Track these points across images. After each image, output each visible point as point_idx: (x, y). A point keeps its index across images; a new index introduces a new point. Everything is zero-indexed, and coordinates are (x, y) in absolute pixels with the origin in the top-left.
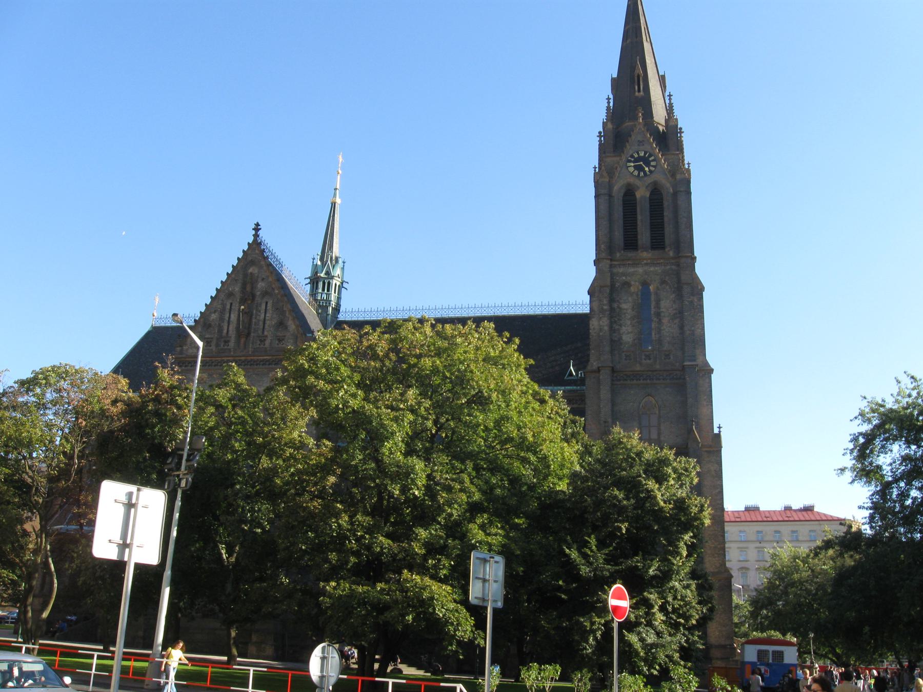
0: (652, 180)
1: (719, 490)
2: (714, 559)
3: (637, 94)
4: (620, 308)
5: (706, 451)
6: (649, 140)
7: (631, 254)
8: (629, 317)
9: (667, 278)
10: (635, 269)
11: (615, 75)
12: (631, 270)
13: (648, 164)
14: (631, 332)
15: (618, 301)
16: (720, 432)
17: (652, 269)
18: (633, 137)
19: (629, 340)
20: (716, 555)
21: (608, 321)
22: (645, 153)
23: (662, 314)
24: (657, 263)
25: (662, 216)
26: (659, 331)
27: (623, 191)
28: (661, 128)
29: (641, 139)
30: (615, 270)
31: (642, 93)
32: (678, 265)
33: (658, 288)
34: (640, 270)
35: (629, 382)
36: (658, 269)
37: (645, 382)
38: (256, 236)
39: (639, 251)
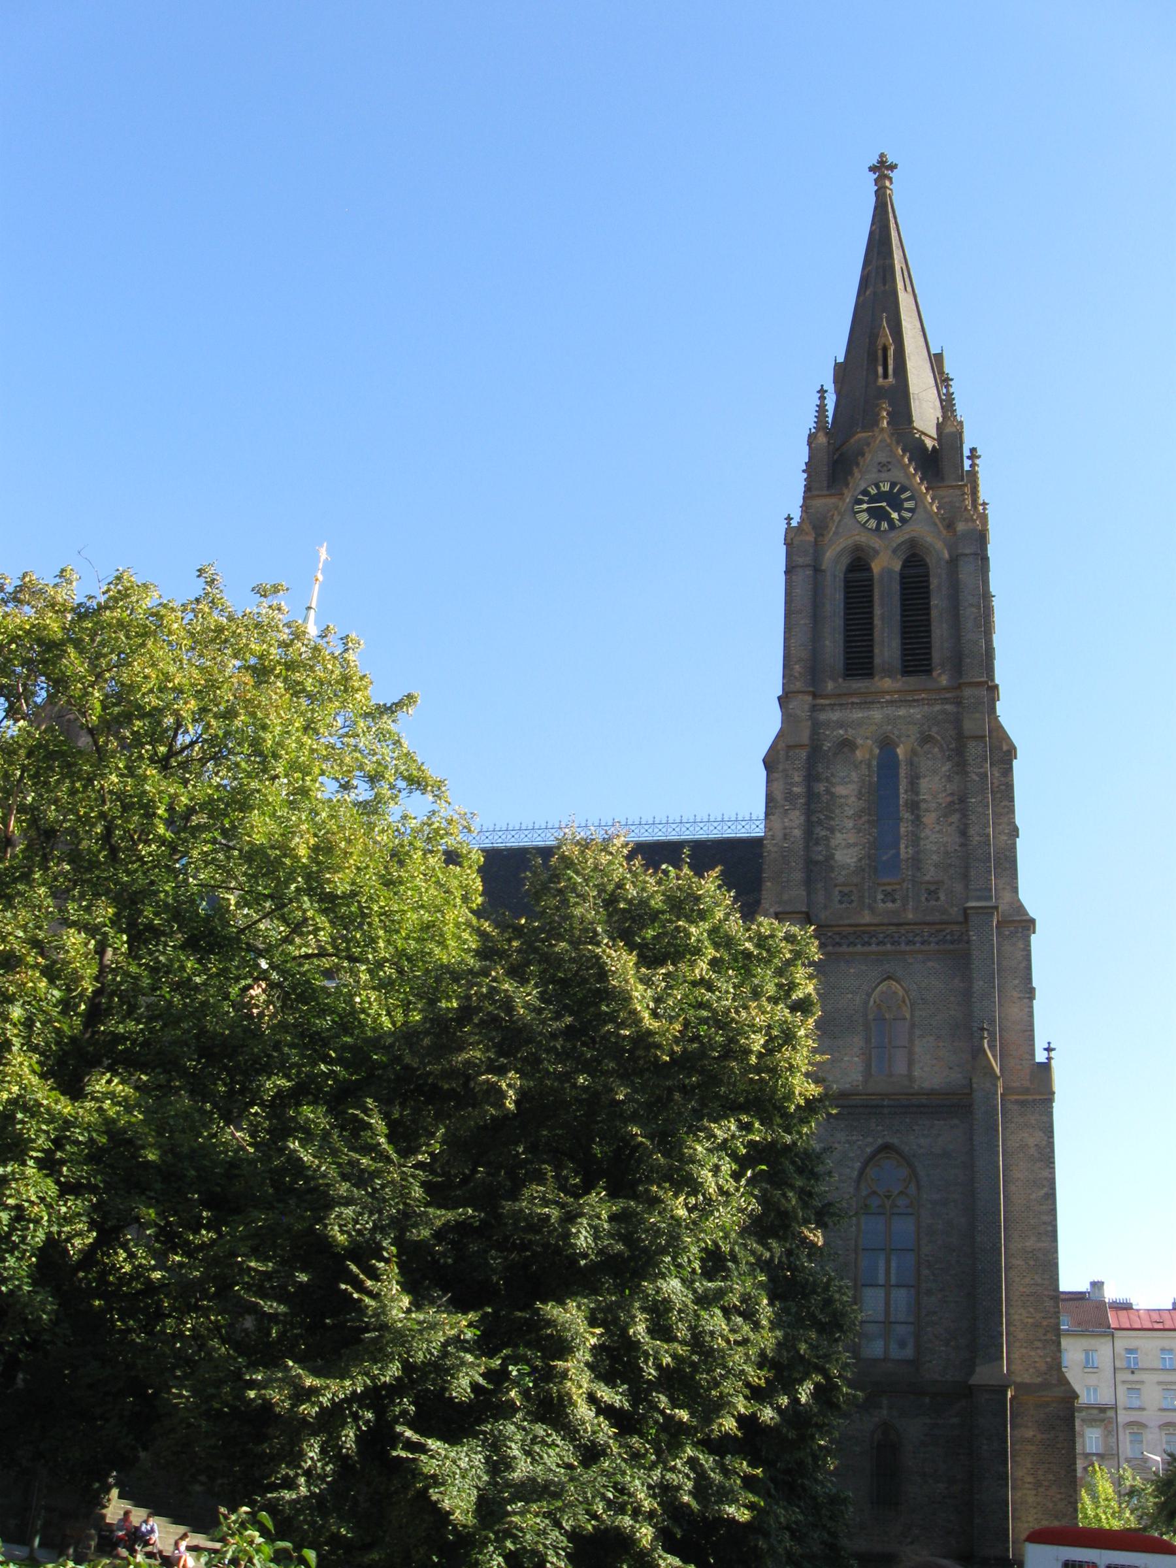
0: (907, 537)
1: (1045, 1190)
2: (1033, 1353)
3: (881, 380)
4: (832, 794)
5: (1017, 1102)
6: (900, 461)
7: (858, 685)
8: (852, 812)
9: (935, 729)
11: (841, 359)
12: (858, 715)
13: (897, 506)
14: (855, 845)
15: (827, 779)
16: (1049, 1059)
17: (902, 712)
18: (868, 457)
19: (849, 861)
21: (803, 818)
22: (893, 485)
23: (923, 806)
24: (914, 701)
25: (927, 609)
26: (915, 840)
27: (845, 561)
28: (929, 444)
29: (884, 460)
30: (823, 717)
31: (891, 379)
32: (958, 702)
33: (914, 752)
34: (877, 715)
35: (844, 949)
36: (916, 712)
37: (881, 948)
39: (877, 678)
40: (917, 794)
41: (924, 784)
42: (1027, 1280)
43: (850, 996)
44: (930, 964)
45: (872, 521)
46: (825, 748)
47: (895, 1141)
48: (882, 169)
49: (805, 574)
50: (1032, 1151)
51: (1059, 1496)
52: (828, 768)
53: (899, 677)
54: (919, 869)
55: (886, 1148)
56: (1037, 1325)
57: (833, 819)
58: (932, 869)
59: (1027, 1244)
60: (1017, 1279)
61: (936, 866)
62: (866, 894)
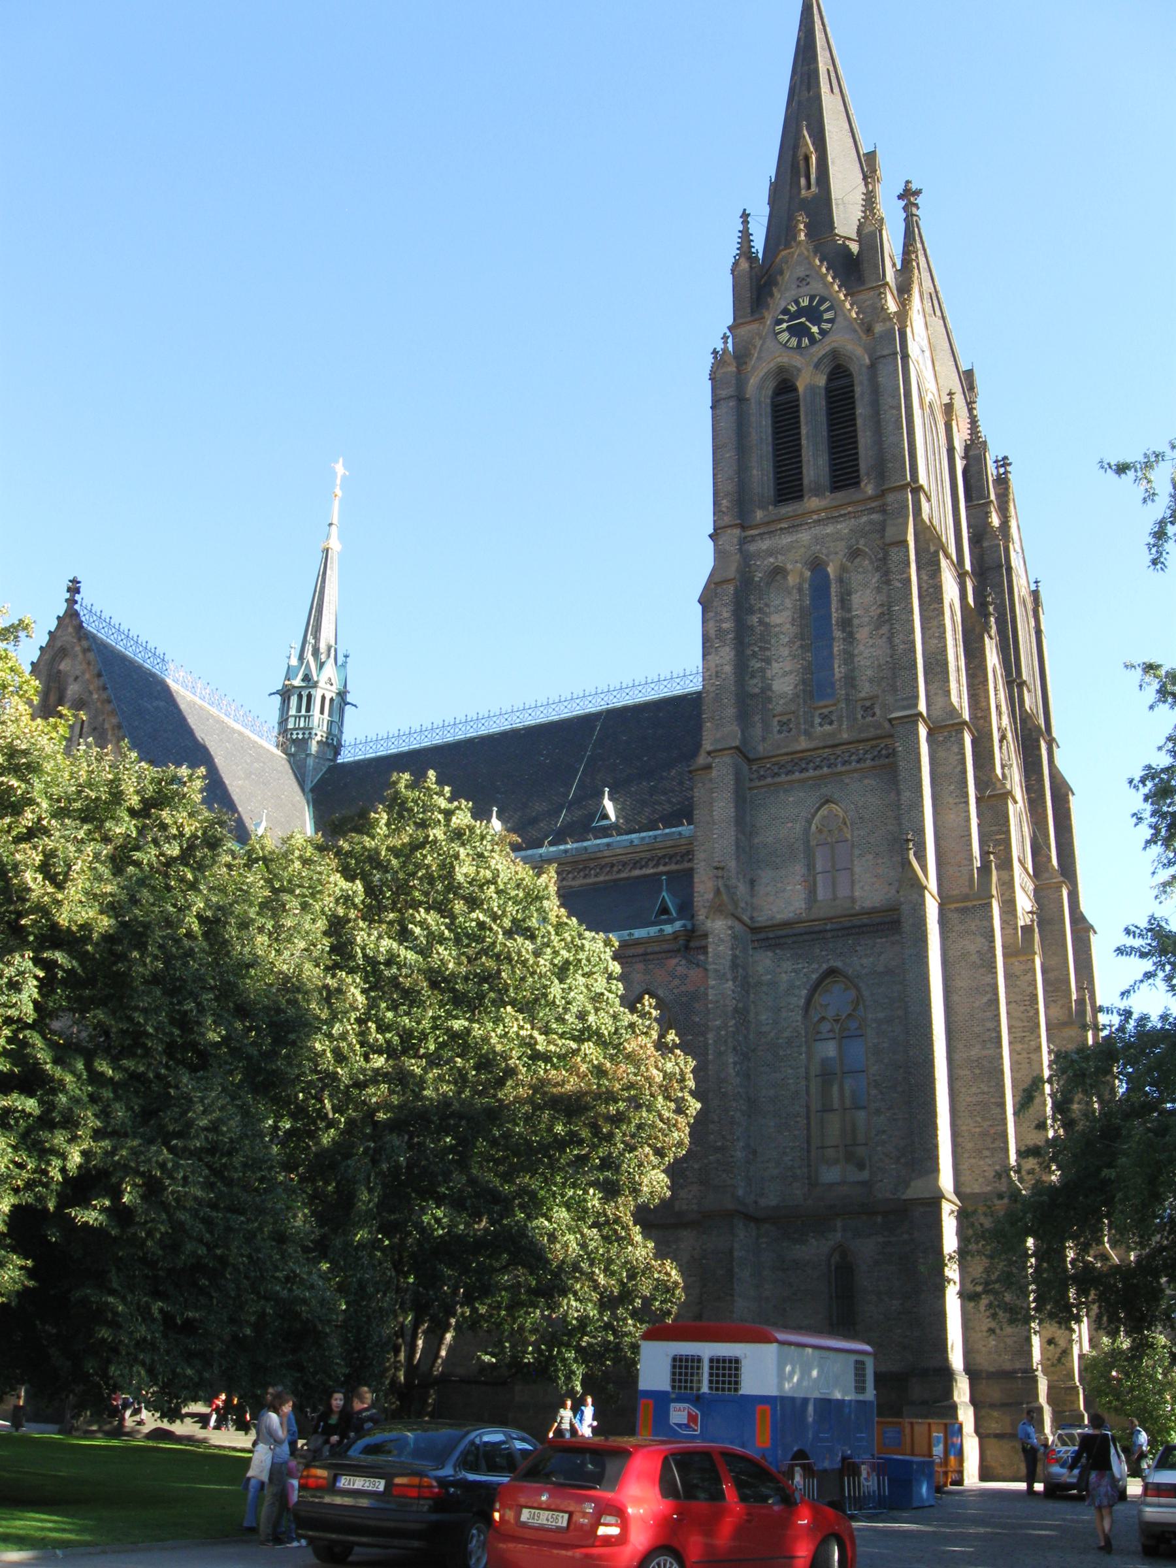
0: (828, 349)
1: (988, 996)
2: (982, 1163)
3: (803, 192)
4: (767, 625)
5: (957, 909)
6: (818, 272)
7: (787, 509)
8: (787, 639)
9: (862, 541)
10: (794, 538)
12: (786, 540)
13: (816, 319)
14: (791, 672)
15: (760, 609)
17: (829, 529)
18: (787, 275)
20: (986, 1153)
21: (733, 653)
22: (812, 298)
23: (856, 622)
24: (841, 516)
25: (852, 419)
26: (849, 657)
27: (771, 385)
28: (854, 247)
29: (802, 275)
30: (752, 548)
31: (814, 189)
32: (883, 510)
33: (843, 569)
34: (805, 536)
35: (783, 778)
36: (843, 527)
37: (818, 773)
38: (71, 602)
39: (806, 500)
40: (849, 610)
41: (856, 599)
42: (974, 1090)
43: (790, 825)
44: (866, 781)
45: (793, 339)
46: (757, 579)
47: (838, 964)
49: (729, 406)
50: (974, 958)
52: (760, 599)
53: (828, 494)
54: (854, 687)
55: (832, 972)
56: (984, 1134)
57: (768, 649)
58: (867, 684)
59: (973, 1053)
60: (963, 1090)
61: (871, 681)
62: (802, 721)
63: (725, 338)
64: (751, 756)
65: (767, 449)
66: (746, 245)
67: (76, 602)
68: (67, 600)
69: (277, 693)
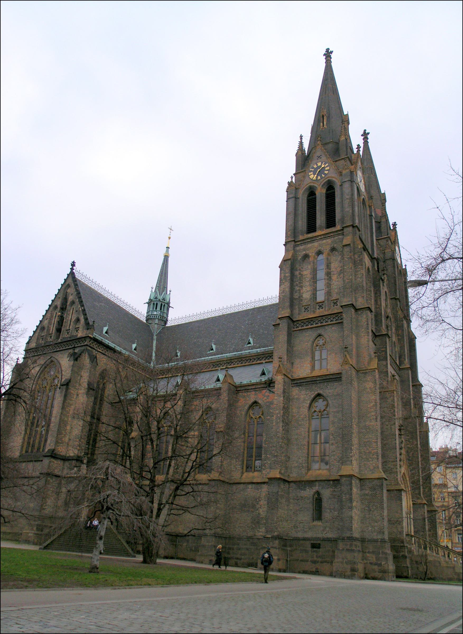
4: (302, 275)
7: (311, 235)
10: (312, 245)
12: (309, 245)
14: (309, 291)
15: (300, 269)
17: (324, 241)
19: (307, 297)
23: (332, 273)
30: (298, 248)
34: (316, 244)
38: (72, 269)
40: (330, 269)
41: (332, 265)
43: (307, 343)
44: (333, 328)
46: (299, 259)
47: (321, 392)
48: (328, 54)
50: (368, 390)
51: (377, 514)
52: (300, 266)
53: (324, 229)
54: (330, 295)
55: (319, 395)
57: (302, 283)
58: (335, 295)
61: (337, 293)
63: (292, 177)
64: (294, 320)
65: (305, 215)
66: (301, 146)
67: (74, 269)
68: (71, 269)
69: (147, 303)
